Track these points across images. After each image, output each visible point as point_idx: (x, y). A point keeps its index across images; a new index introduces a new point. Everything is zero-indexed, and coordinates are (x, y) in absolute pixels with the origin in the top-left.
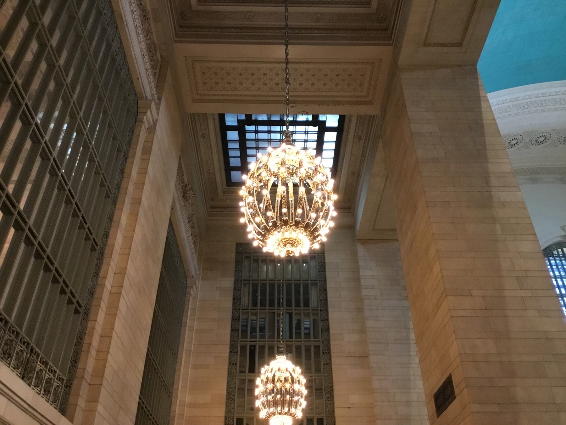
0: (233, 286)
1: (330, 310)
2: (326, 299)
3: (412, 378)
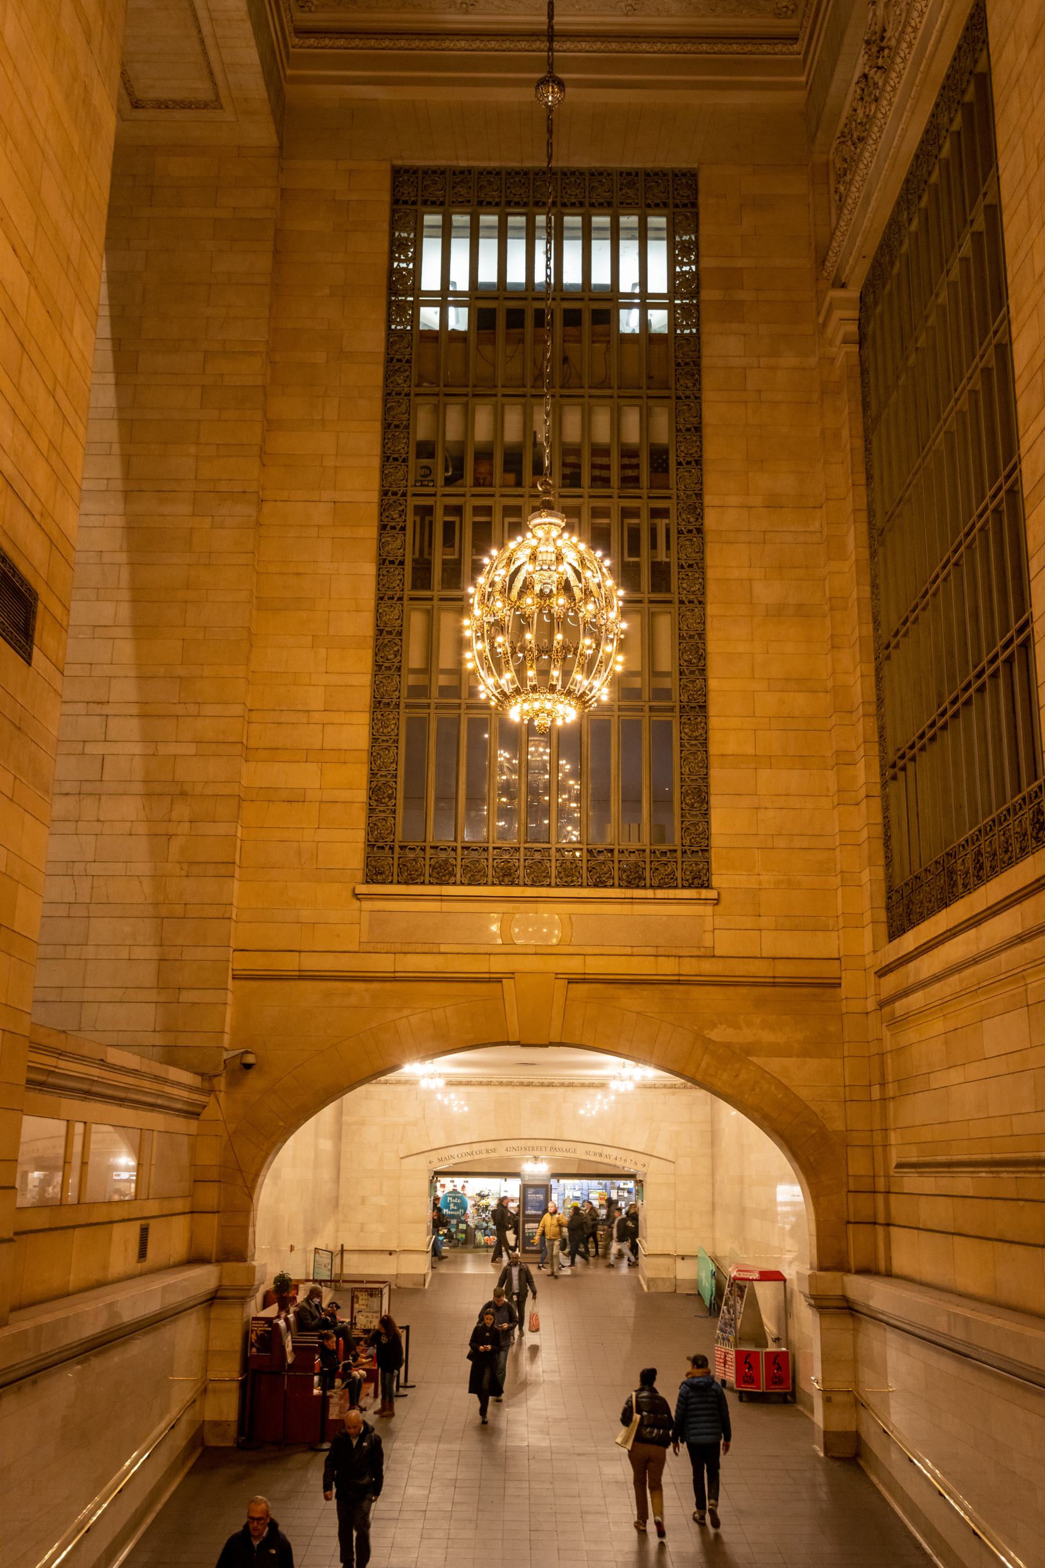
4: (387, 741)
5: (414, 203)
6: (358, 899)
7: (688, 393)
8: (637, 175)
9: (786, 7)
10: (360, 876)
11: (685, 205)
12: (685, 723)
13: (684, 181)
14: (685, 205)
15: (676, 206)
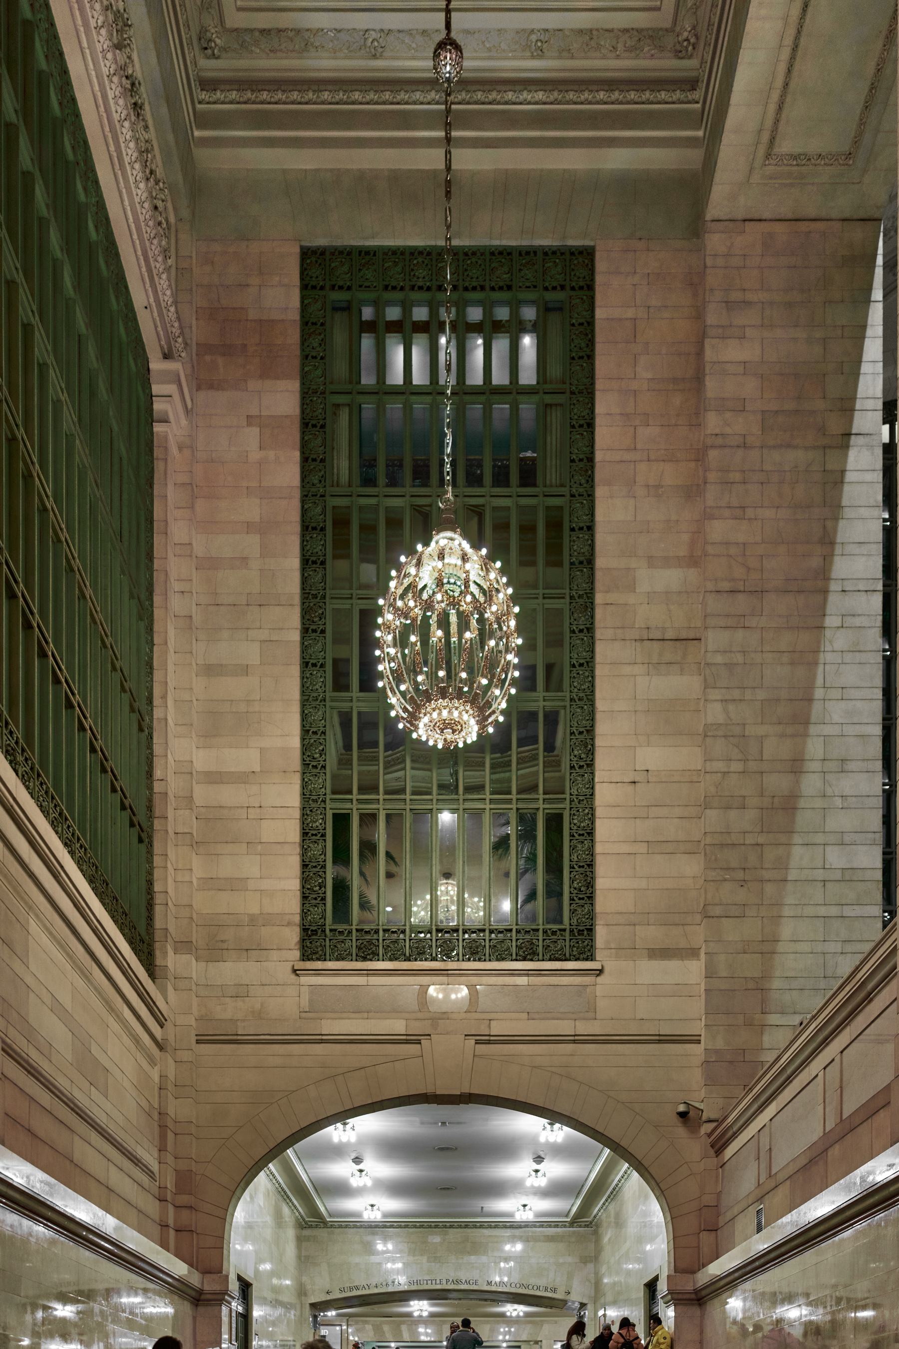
0: (297, 411)
1: (600, 492)
2: (591, 459)
3: (819, 693)
4: (316, 835)
5: (322, 288)
6: (297, 975)
7: (581, 490)
8: (535, 253)
9: (687, 40)
10: (297, 954)
11: (581, 288)
12: (574, 815)
13: (581, 260)
14: (581, 288)
15: (573, 288)
